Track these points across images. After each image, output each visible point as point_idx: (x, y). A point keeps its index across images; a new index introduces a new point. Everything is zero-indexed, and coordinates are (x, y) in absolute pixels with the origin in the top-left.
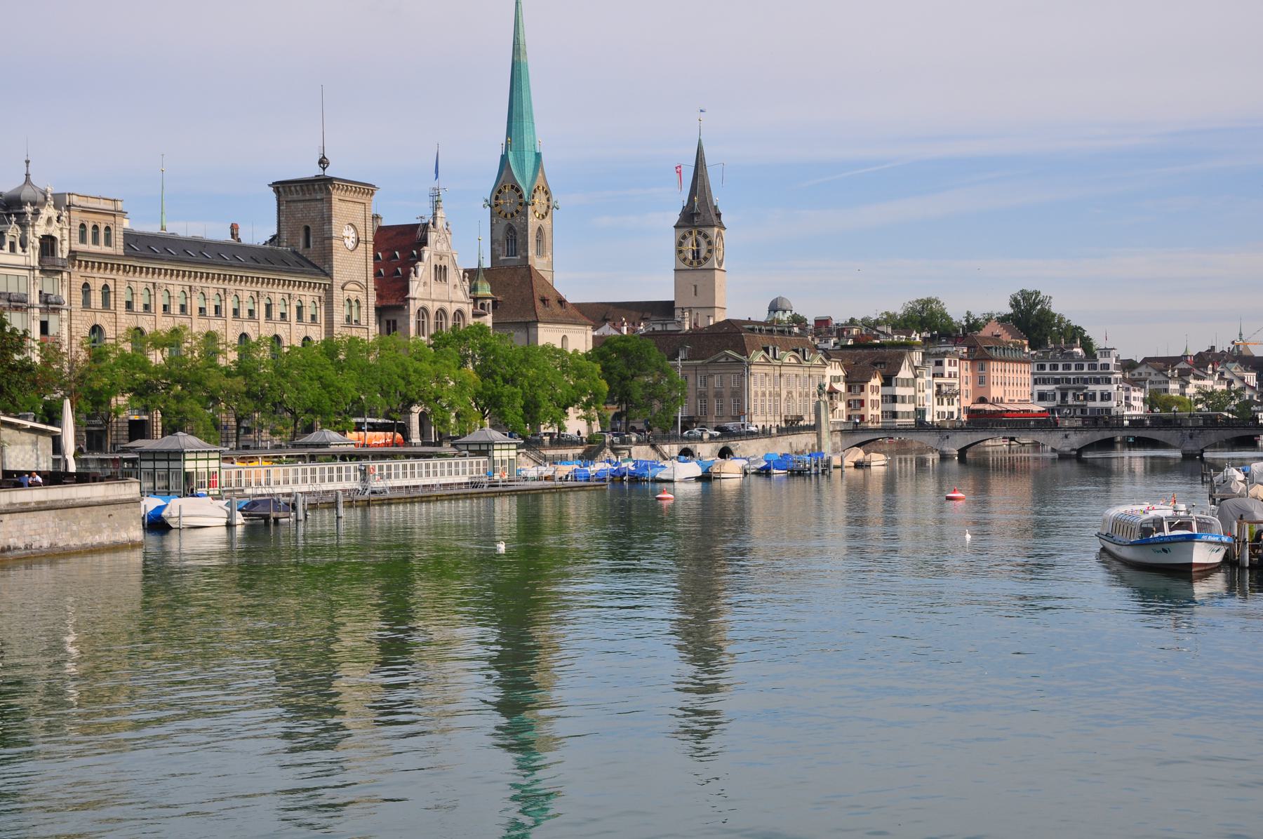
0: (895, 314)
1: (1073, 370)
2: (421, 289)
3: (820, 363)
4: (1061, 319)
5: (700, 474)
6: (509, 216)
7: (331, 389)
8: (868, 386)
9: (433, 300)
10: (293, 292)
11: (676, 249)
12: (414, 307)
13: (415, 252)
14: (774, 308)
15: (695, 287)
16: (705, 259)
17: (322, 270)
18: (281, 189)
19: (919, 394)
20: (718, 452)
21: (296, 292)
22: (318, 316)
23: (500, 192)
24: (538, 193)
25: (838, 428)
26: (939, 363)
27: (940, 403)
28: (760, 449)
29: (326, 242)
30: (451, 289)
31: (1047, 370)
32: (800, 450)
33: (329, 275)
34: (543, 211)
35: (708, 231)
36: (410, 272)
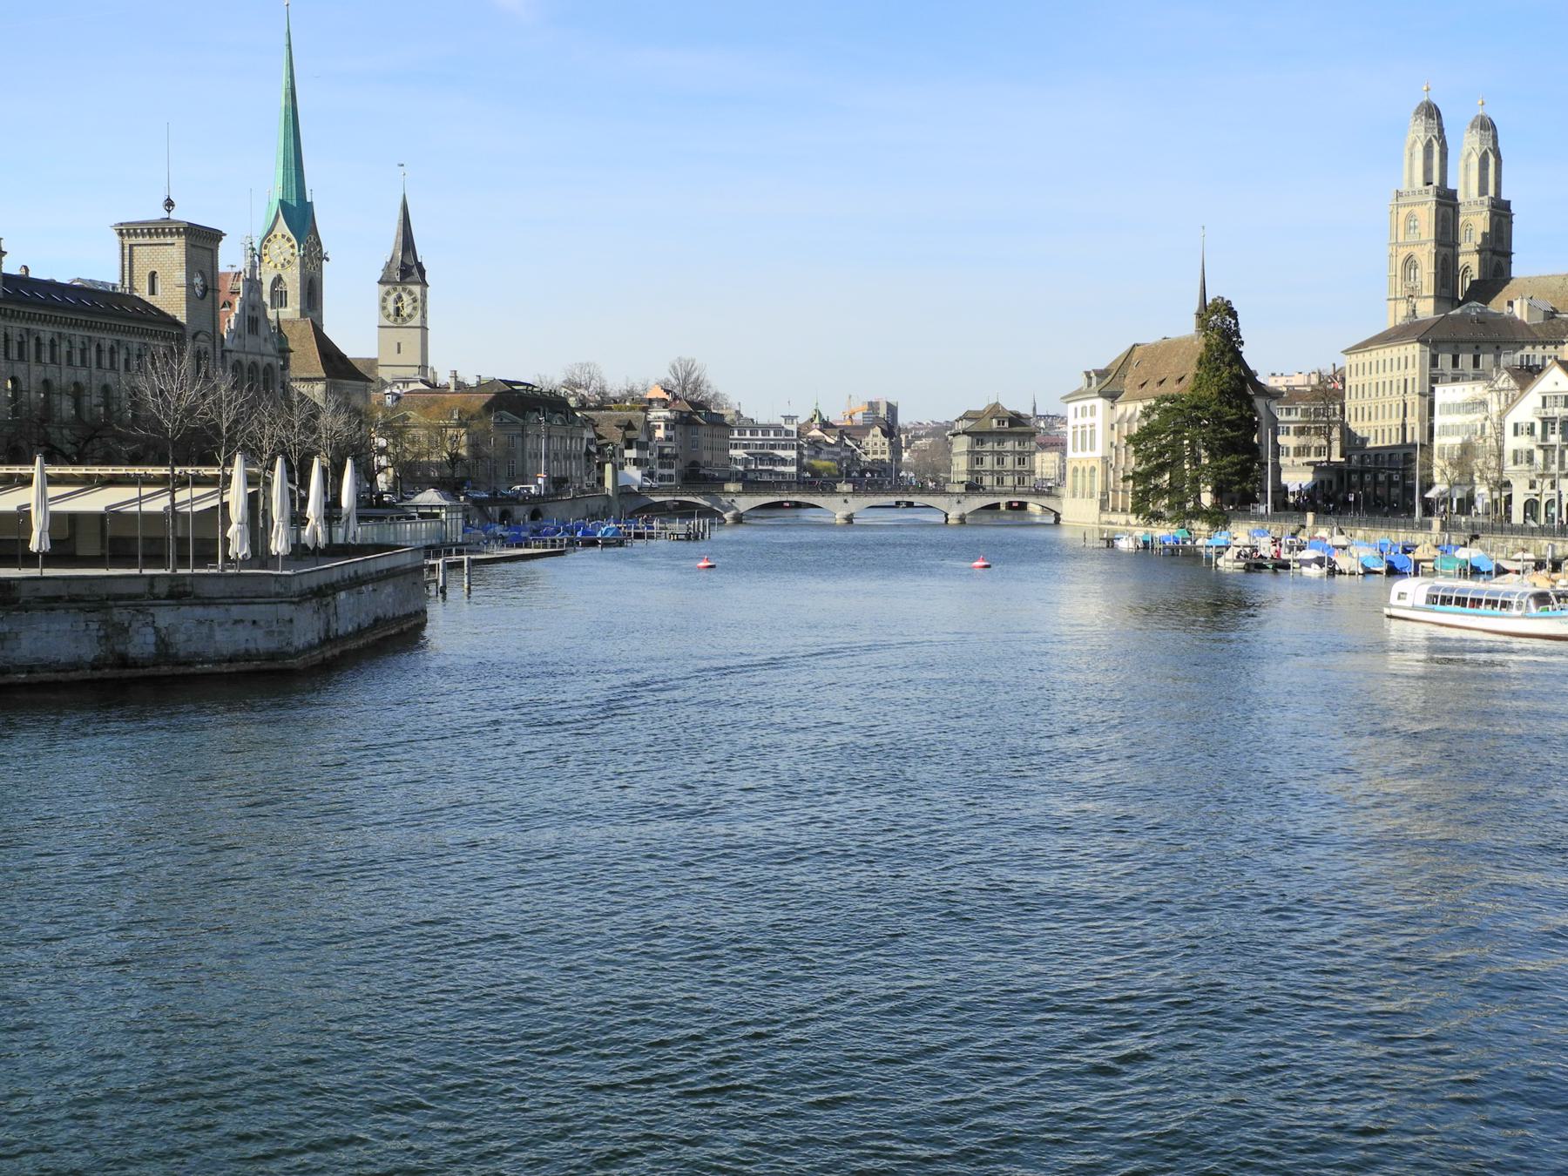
1: (760, 436)
15: (399, 344)
16: (410, 316)
30: (262, 341)
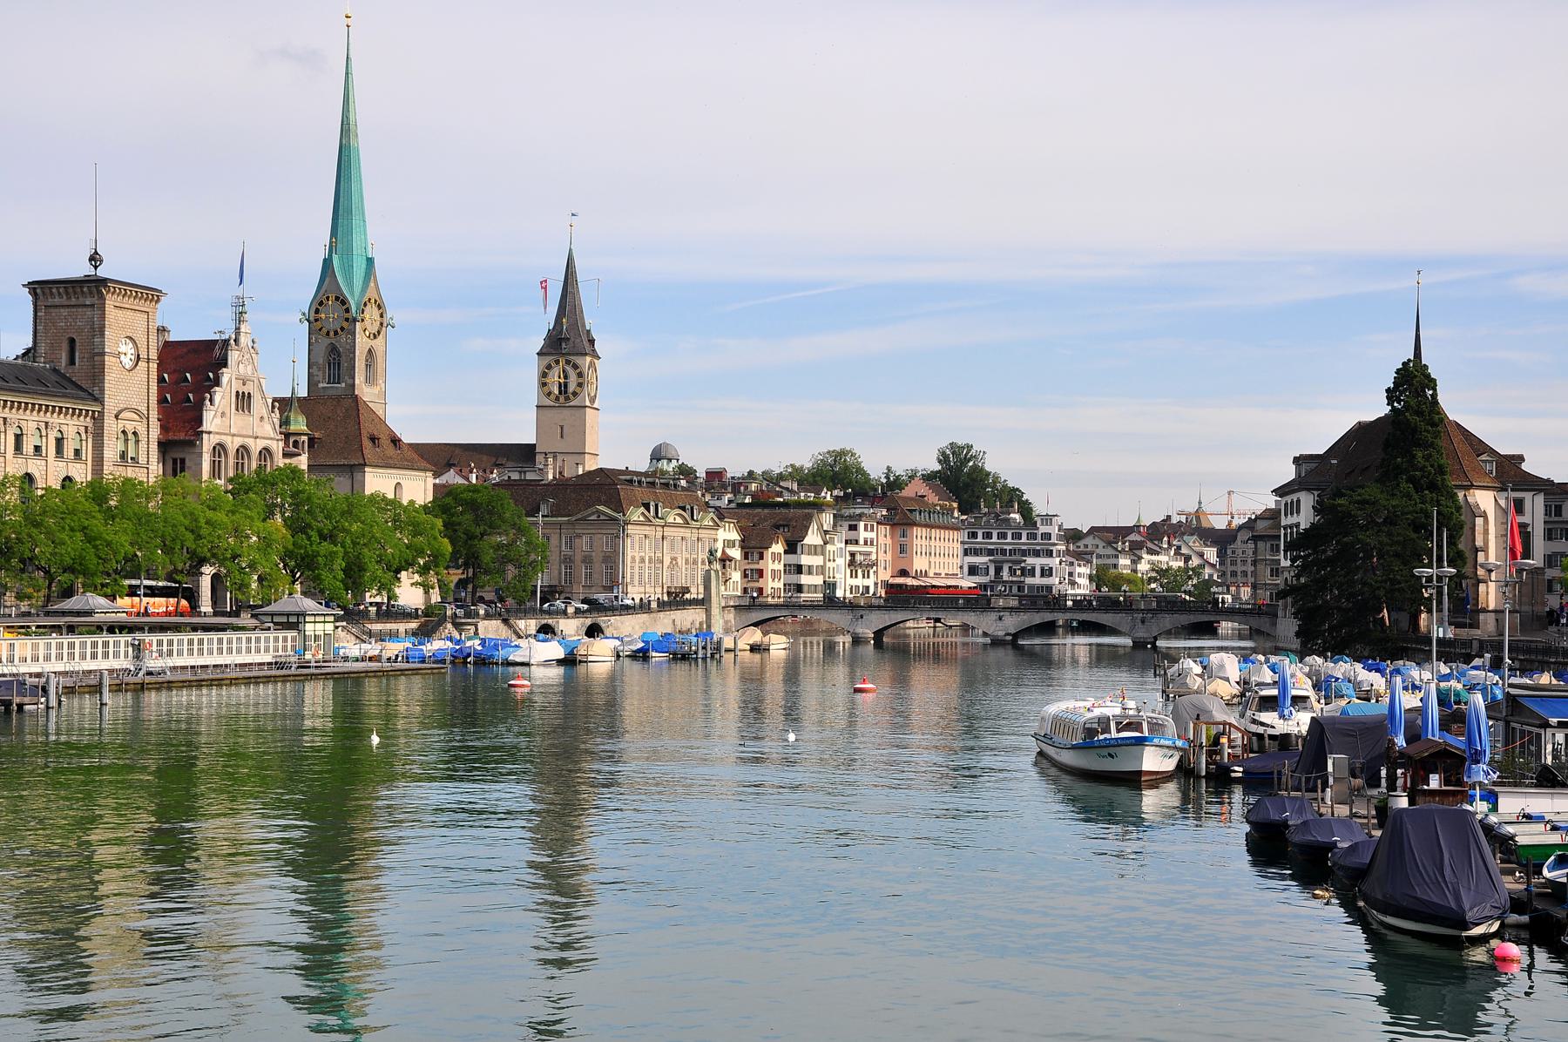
0: (802, 467)
1: (1009, 540)
2: (218, 421)
3: (711, 524)
4: (996, 478)
5: (563, 657)
6: (332, 333)
7: (98, 542)
8: (768, 554)
9: (234, 435)
10: (51, 420)
11: (539, 380)
12: (208, 443)
13: (211, 375)
14: (657, 455)
15: (562, 427)
16: (575, 394)
17: (90, 394)
18: (38, 291)
19: (828, 564)
20: (585, 629)
21: (54, 419)
22: (84, 452)
23: (321, 303)
24: (369, 305)
25: (732, 604)
26: (853, 528)
27: (854, 575)
28: (637, 627)
29: (96, 358)
30: (257, 421)
31: (980, 539)
32: (684, 629)
33: (99, 400)
34: (375, 330)
35: (578, 360)
36: (204, 399)
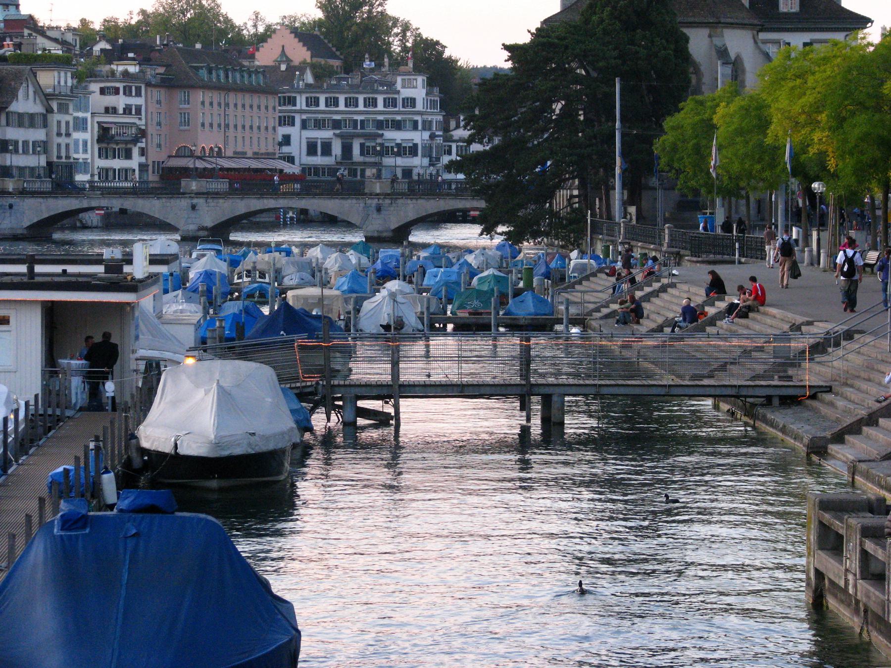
1: (361, 107)
4: (406, 27)
27: (103, 154)
